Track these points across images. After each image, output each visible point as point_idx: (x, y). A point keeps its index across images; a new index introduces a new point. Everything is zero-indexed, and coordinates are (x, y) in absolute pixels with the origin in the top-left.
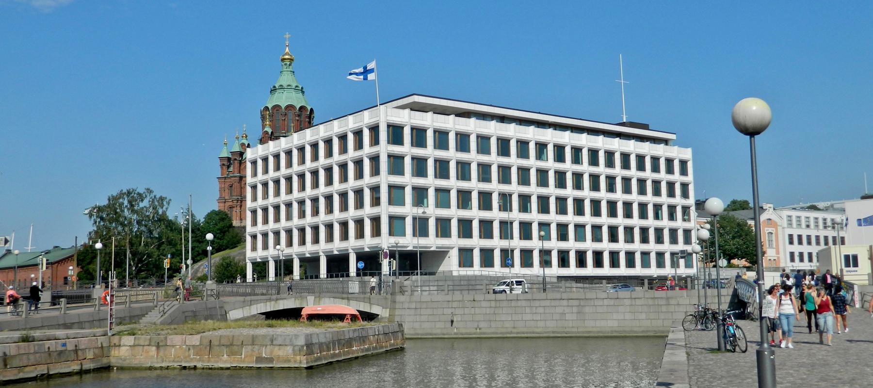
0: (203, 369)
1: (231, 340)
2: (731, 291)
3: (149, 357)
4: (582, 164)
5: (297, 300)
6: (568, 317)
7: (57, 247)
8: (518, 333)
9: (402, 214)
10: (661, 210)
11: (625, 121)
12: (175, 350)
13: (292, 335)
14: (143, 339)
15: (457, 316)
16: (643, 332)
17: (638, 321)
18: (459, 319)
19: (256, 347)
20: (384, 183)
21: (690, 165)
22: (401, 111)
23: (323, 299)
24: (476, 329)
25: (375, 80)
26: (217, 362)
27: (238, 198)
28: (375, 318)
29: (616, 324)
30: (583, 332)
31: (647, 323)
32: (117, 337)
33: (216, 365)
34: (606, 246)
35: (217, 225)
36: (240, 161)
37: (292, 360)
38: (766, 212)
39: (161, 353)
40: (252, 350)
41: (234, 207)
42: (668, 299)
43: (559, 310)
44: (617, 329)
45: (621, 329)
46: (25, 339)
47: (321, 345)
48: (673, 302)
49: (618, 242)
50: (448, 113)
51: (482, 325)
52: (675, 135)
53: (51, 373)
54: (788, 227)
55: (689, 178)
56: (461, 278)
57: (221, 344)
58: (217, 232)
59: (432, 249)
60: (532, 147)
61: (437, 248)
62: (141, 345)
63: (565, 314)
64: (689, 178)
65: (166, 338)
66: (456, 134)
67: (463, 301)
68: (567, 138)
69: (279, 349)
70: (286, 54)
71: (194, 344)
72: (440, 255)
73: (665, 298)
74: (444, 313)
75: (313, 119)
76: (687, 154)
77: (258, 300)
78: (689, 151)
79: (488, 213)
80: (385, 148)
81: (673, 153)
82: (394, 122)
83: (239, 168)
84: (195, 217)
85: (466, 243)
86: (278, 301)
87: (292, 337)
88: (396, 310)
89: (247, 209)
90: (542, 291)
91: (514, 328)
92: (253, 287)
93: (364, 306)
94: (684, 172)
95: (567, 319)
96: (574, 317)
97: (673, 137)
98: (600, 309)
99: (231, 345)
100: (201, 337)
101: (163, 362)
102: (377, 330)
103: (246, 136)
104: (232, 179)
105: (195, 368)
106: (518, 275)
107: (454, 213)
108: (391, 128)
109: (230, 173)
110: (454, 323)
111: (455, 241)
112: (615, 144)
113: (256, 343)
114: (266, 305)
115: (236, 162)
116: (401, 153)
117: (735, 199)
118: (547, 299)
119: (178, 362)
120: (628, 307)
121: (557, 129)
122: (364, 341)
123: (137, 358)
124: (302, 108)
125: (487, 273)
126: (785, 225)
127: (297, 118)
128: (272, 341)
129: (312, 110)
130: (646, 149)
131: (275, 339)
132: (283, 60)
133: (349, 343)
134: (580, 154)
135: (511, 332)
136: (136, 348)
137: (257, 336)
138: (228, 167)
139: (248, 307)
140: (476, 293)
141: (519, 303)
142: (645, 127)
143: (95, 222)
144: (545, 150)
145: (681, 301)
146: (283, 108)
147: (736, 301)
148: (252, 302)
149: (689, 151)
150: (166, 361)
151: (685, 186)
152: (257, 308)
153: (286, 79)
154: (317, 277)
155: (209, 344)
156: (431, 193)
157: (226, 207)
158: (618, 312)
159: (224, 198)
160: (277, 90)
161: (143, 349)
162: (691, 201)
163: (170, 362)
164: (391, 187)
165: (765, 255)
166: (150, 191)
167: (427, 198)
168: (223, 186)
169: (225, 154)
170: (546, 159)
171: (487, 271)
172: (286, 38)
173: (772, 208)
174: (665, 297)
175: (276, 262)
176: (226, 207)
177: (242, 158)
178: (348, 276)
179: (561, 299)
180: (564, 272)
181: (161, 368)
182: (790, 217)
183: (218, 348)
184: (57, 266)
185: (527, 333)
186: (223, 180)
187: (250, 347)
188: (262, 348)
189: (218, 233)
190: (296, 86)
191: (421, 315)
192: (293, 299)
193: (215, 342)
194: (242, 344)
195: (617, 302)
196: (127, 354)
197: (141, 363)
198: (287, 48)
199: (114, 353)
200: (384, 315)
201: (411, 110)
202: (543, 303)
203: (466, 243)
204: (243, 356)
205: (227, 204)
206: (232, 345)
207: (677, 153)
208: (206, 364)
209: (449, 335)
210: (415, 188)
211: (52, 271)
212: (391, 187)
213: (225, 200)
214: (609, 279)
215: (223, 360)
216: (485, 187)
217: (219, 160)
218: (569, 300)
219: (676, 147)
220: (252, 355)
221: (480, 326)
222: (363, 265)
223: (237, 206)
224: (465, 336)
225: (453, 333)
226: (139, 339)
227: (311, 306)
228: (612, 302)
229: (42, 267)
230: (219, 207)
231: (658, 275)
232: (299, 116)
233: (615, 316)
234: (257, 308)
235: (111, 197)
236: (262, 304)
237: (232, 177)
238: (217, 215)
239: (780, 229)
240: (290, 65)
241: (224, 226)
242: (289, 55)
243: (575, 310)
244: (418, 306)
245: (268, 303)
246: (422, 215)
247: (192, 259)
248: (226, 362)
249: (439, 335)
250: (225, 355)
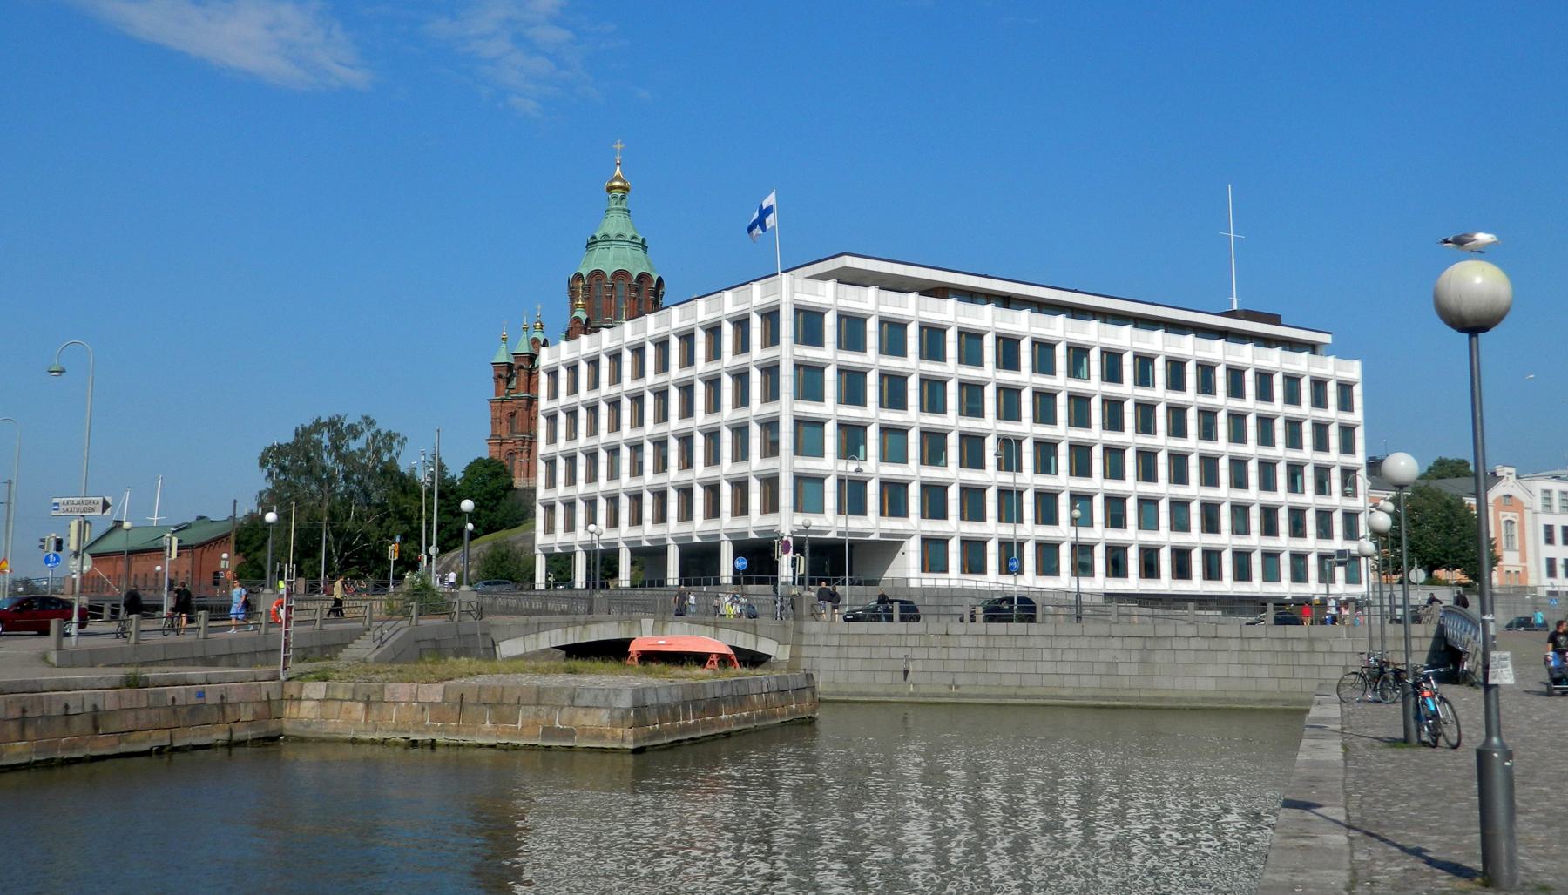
0: (448, 745)
1: (498, 695)
2: (1432, 630)
3: (351, 719)
4: (1154, 386)
5: (622, 625)
6: (1122, 669)
7: (202, 518)
8: (1029, 697)
9: (818, 472)
10: (1302, 473)
11: (1235, 308)
12: (398, 711)
13: (609, 689)
14: (341, 689)
15: (914, 662)
16: (1263, 701)
17: (1254, 680)
18: (920, 668)
19: (543, 708)
20: (786, 415)
21: (1357, 391)
22: (820, 284)
23: (670, 624)
24: (950, 687)
25: (774, 227)
26: (473, 734)
27: (524, 438)
28: (762, 662)
30: (1149, 699)
31: (1270, 686)
32: (294, 683)
33: (471, 740)
34: (1195, 538)
35: (486, 485)
36: (530, 370)
37: (609, 735)
38: (1502, 483)
39: (374, 712)
40: (537, 715)
41: (517, 453)
42: (1311, 640)
43: (1104, 656)
44: (1211, 695)
45: (1221, 695)
46: (132, 683)
47: (661, 708)
48: (1320, 646)
49: (1220, 533)
50: (906, 289)
51: (960, 680)
52: (1330, 336)
53: (177, 744)
54: (1544, 512)
55: (1357, 416)
56: (926, 592)
57: (481, 701)
58: (486, 497)
59: (872, 538)
60: (1061, 353)
61: (882, 535)
62: (339, 700)
63: (1117, 663)
64: (1357, 416)
65: (382, 688)
66: (920, 327)
67: (926, 634)
68: (1125, 338)
69: (586, 714)
70: (616, 179)
71: (432, 699)
72: (889, 547)
73: (1305, 639)
74: (892, 656)
75: (662, 296)
76: (1352, 371)
77: (550, 623)
78: (1356, 366)
79: (978, 474)
80: (788, 352)
81: (1326, 368)
82: (808, 304)
83: (527, 384)
84: (446, 469)
85: (934, 527)
86: (588, 626)
87: (609, 693)
88: (804, 648)
89: (538, 457)
90: (1075, 621)
91: (1021, 687)
92: (544, 597)
93: (745, 639)
94: (1346, 404)
95: (1119, 673)
96: (1134, 669)
97: (1327, 339)
98: (1181, 657)
99: (499, 704)
100: (445, 687)
101: (376, 731)
102: (765, 684)
103: (542, 326)
104: (514, 402)
105: (433, 744)
106: (1031, 590)
107: (913, 471)
108: (801, 314)
109: (511, 391)
110: (910, 675)
111: (914, 524)
112: (1218, 352)
113: (543, 702)
114: (567, 631)
115: (522, 371)
116: (818, 361)
117: (1443, 457)
118: (1083, 636)
119: (402, 731)
120: (1236, 653)
121: (1108, 320)
122: (741, 704)
123: (330, 723)
124: (643, 277)
125: (973, 584)
127: (633, 295)
128: (573, 701)
129: (660, 280)
130: (1274, 359)
131: (579, 695)
132: (610, 189)
133: (714, 706)
134: (1150, 367)
135: (1016, 694)
136: (329, 704)
137: (545, 690)
138: (509, 381)
139: (533, 636)
140: (952, 621)
141: (1031, 642)
142: (1274, 319)
143: (270, 474)
144: (1085, 359)
145: (1337, 647)
146: (609, 275)
147: (1443, 648)
148: (542, 627)
149: (1356, 366)
150: (381, 729)
151: (1347, 431)
152: (550, 638)
153: (614, 224)
154: (662, 583)
155: (458, 700)
156: (873, 434)
157: (503, 453)
158: (1216, 664)
159: (500, 436)
160: (599, 243)
161: (341, 706)
162: (1359, 459)
163: (388, 731)
164: (799, 422)
165: (1500, 563)
166: (369, 422)
167: (865, 443)
168: (498, 415)
169: (503, 357)
170: (1086, 377)
171: (973, 581)
172: (616, 149)
173: (1514, 475)
174: (1306, 635)
175: (588, 554)
176: (503, 453)
177: (533, 365)
178: (717, 582)
179: (1110, 636)
180: (1117, 585)
181: (373, 742)
182: (1548, 492)
183: (475, 708)
184: (202, 552)
185: (1045, 697)
186: (499, 404)
187: (532, 709)
188: (553, 711)
189: (486, 499)
190: (633, 237)
191: (848, 658)
192: (616, 623)
193: (470, 698)
194: (519, 703)
195: (1214, 644)
196: (312, 715)
197: (337, 731)
198: (618, 168)
199: (290, 713)
200: (780, 658)
202: (1076, 643)
203: (934, 527)
204: (520, 725)
205: (506, 448)
206: (500, 703)
207: (1331, 368)
208: (453, 738)
209: (900, 696)
210: (842, 426)
211: (193, 561)
212: (799, 422)
213: (502, 440)
214: (1203, 601)
215: (483, 732)
216: (972, 425)
217: (492, 366)
218: (1125, 639)
219: (1331, 359)
220: (535, 724)
221: (958, 683)
222: (746, 563)
223: (521, 452)
224: (930, 700)
225: (907, 693)
226: (335, 687)
227: (647, 637)
228: (1205, 644)
229: (170, 554)
230: (490, 452)
231: (1294, 595)
232: (636, 290)
233: (1211, 670)
234: (550, 638)
235: (300, 429)
236: (560, 630)
237: (514, 398)
238: (486, 466)
239: (1528, 515)
240: (622, 198)
241: (498, 487)
242: (621, 180)
243: (1135, 656)
244: (844, 642)
245: (570, 630)
246: (855, 474)
247: (438, 545)
248: (489, 734)
249: (880, 695)
250: (488, 722)
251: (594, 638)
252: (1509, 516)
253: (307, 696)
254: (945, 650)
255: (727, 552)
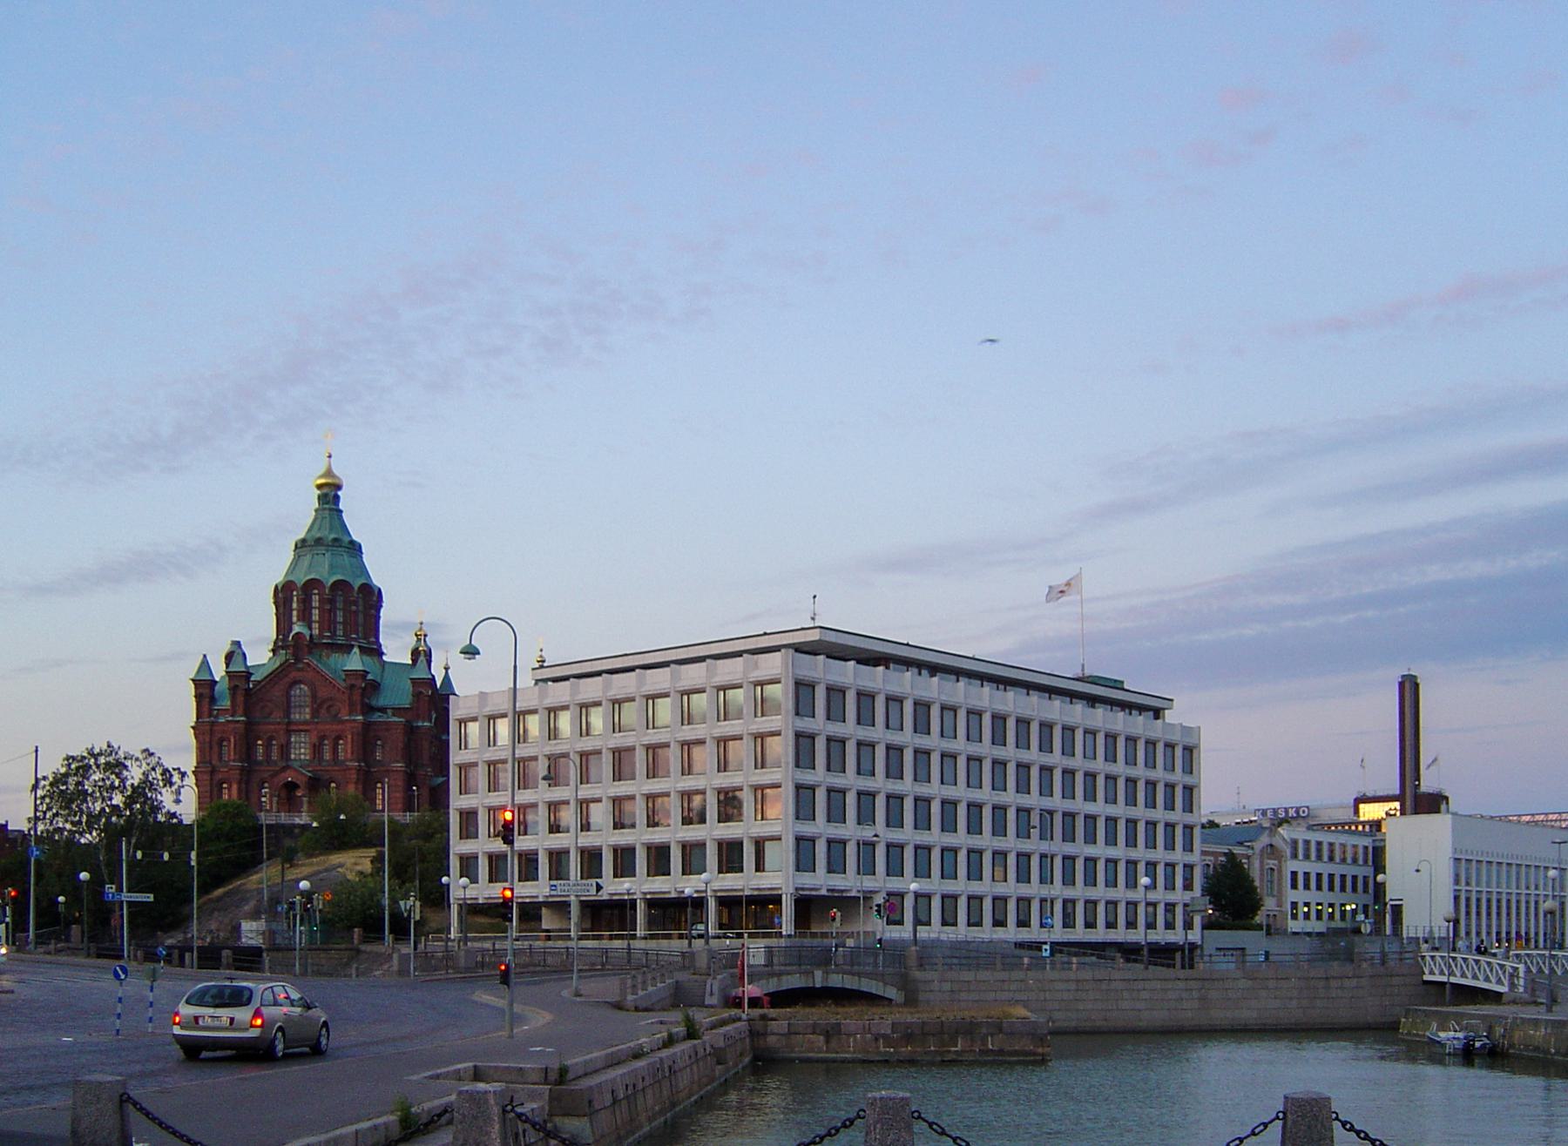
12: (855, 1040)
29: (1255, 1015)
51: (1057, 1015)
74: (998, 998)
126: (1288, 854)
129: (380, 590)
136: (793, 1037)
141: (1114, 985)
201: (828, 657)
202: (1148, 985)
243: (1195, 994)
245: (771, 980)
251: (784, 988)
252: (1272, 863)
253: (771, 1030)
254: (1042, 994)
255: (712, 905)
